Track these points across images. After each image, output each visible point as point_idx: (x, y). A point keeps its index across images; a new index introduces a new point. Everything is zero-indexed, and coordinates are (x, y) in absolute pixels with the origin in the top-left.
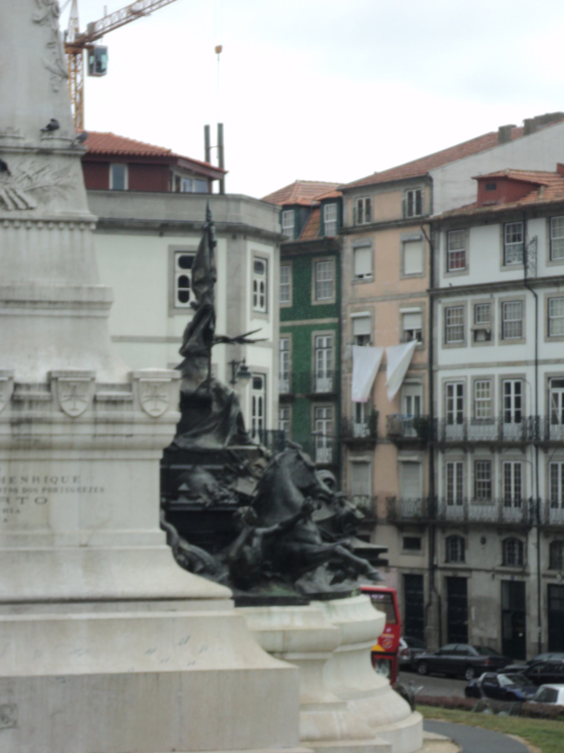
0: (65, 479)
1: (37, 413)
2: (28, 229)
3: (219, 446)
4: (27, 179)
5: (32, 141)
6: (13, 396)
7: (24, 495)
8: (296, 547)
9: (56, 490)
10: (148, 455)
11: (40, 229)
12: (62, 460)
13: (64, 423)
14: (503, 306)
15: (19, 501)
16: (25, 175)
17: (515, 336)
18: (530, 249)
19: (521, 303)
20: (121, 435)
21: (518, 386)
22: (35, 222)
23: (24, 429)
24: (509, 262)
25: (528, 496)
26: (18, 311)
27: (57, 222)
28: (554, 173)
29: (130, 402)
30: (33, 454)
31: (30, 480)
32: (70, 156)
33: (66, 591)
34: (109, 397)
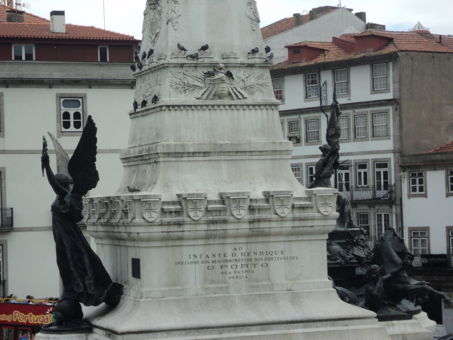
0: (277, 253)
1: (263, 215)
2: (244, 110)
3: (343, 229)
4: (241, 81)
5: (242, 59)
6: (250, 206)
7: (255, 263)
8: (400, 286)
9: (272, 259)
10: (320, 237)
11: (250, 109)
12: (274, 242)
13: (277, 221)
14: (306, 122)
15: (253, 265)
16: (241, 79)
17: (315, 140)
18: (323, 88)
20: (308, 226)
22: (248, 106)
23: (256, 225)
24: (310, 96)
26: (242, 157)
27: (259, 105)
28: (331, 43)
29: (312, 207)
30: (260, 239)
31: (258, 254)
32: (264, 67)
33: (289, 317)
34: (301, 205)
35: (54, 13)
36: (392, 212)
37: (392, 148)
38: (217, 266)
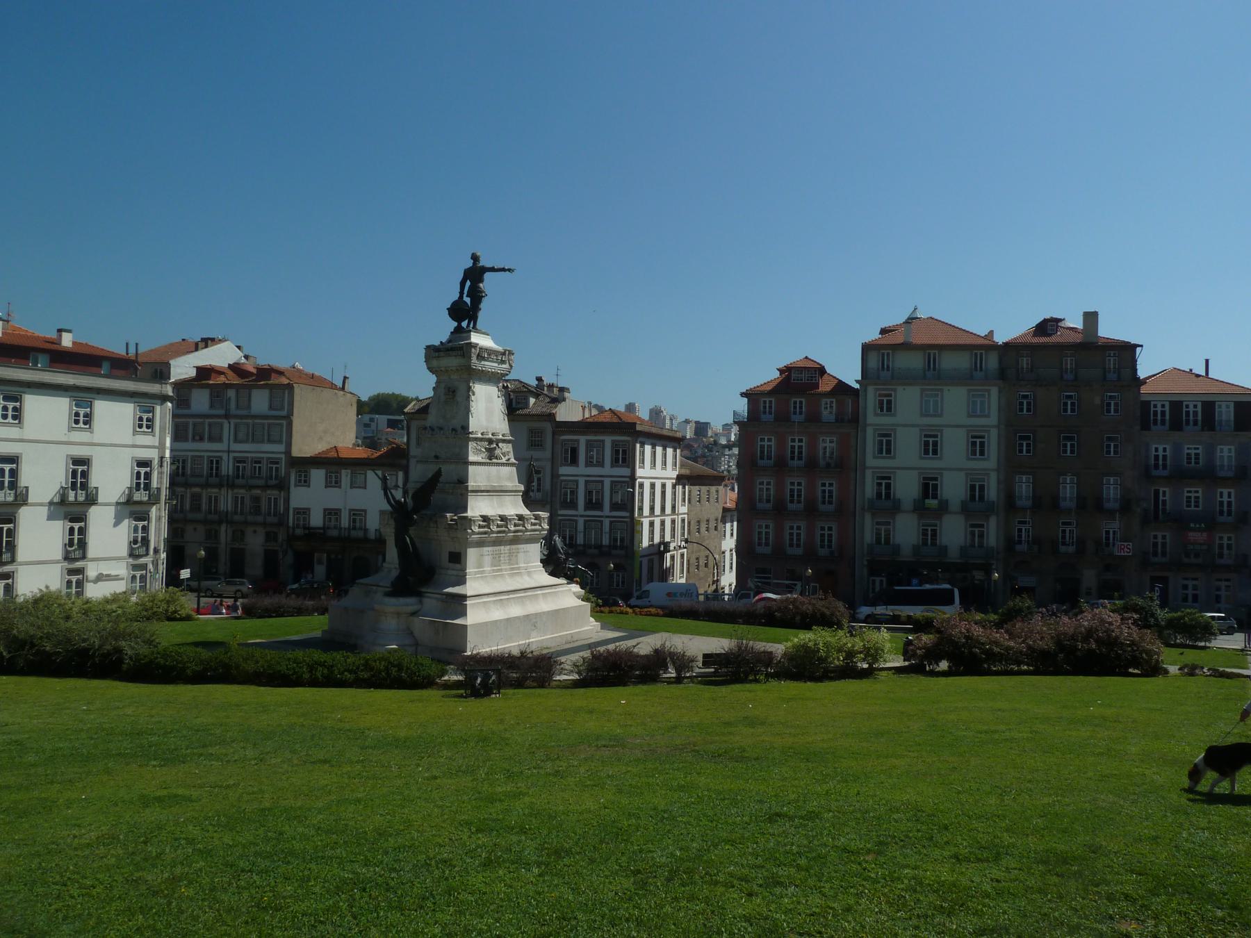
14: (210, 425)
19: (221, 425)
21: (217, 462)
25: (222, 509)
35: (60, 331)
36: (280, 497)
37: (284, 451)
38: (497, 556)
